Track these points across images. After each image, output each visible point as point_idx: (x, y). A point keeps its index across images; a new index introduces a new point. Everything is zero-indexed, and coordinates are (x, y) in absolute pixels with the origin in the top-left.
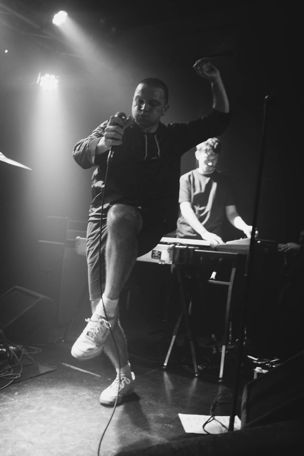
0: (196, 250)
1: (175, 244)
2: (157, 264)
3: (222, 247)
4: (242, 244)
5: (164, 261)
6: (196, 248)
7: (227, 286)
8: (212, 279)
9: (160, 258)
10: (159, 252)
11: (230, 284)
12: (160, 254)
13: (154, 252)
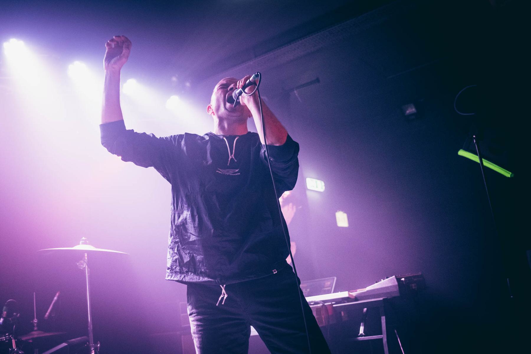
0: (334, 306)
3: (363, 295)
4: (384, 286)
6: (333, 303)
7: (381, 340)
8: (362, 335)
11: (384, 337)
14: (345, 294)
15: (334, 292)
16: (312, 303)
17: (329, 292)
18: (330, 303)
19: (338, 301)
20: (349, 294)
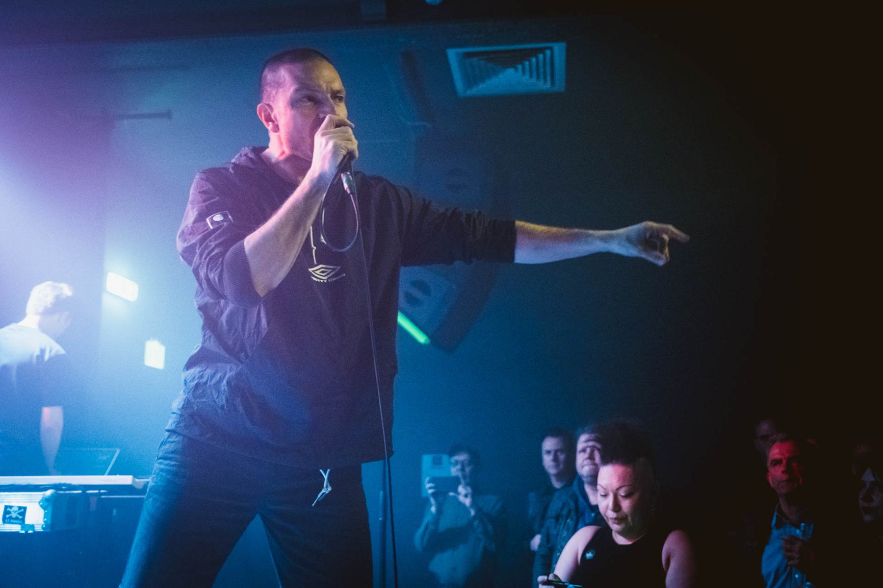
1: (56, 487)
2: (16, 534)
5: (32, 527)
6: (102, 491)
9: (23, 520)
10: (20, 508)
12: (23, 511)
13: (8, 509)
14: (126, 480)
15: (110, 474)
16: (64, 488)
17: (101, 472)
18: (97, 491)
20: (133, 481)
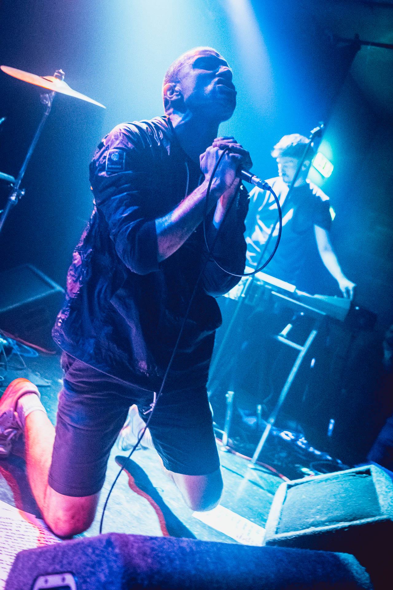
0: (273, 293)
7: (298, 352)
8: (282, 336)
11: (303, 350)
19: (280, 291)
20: (295, 291)
